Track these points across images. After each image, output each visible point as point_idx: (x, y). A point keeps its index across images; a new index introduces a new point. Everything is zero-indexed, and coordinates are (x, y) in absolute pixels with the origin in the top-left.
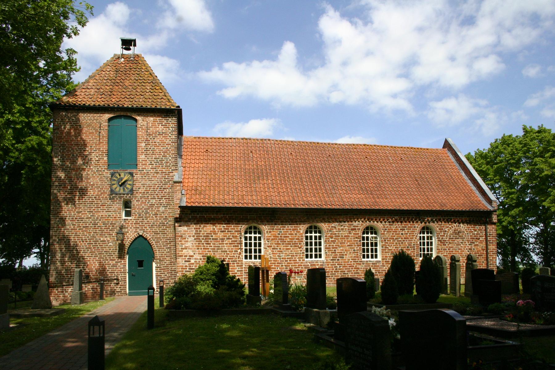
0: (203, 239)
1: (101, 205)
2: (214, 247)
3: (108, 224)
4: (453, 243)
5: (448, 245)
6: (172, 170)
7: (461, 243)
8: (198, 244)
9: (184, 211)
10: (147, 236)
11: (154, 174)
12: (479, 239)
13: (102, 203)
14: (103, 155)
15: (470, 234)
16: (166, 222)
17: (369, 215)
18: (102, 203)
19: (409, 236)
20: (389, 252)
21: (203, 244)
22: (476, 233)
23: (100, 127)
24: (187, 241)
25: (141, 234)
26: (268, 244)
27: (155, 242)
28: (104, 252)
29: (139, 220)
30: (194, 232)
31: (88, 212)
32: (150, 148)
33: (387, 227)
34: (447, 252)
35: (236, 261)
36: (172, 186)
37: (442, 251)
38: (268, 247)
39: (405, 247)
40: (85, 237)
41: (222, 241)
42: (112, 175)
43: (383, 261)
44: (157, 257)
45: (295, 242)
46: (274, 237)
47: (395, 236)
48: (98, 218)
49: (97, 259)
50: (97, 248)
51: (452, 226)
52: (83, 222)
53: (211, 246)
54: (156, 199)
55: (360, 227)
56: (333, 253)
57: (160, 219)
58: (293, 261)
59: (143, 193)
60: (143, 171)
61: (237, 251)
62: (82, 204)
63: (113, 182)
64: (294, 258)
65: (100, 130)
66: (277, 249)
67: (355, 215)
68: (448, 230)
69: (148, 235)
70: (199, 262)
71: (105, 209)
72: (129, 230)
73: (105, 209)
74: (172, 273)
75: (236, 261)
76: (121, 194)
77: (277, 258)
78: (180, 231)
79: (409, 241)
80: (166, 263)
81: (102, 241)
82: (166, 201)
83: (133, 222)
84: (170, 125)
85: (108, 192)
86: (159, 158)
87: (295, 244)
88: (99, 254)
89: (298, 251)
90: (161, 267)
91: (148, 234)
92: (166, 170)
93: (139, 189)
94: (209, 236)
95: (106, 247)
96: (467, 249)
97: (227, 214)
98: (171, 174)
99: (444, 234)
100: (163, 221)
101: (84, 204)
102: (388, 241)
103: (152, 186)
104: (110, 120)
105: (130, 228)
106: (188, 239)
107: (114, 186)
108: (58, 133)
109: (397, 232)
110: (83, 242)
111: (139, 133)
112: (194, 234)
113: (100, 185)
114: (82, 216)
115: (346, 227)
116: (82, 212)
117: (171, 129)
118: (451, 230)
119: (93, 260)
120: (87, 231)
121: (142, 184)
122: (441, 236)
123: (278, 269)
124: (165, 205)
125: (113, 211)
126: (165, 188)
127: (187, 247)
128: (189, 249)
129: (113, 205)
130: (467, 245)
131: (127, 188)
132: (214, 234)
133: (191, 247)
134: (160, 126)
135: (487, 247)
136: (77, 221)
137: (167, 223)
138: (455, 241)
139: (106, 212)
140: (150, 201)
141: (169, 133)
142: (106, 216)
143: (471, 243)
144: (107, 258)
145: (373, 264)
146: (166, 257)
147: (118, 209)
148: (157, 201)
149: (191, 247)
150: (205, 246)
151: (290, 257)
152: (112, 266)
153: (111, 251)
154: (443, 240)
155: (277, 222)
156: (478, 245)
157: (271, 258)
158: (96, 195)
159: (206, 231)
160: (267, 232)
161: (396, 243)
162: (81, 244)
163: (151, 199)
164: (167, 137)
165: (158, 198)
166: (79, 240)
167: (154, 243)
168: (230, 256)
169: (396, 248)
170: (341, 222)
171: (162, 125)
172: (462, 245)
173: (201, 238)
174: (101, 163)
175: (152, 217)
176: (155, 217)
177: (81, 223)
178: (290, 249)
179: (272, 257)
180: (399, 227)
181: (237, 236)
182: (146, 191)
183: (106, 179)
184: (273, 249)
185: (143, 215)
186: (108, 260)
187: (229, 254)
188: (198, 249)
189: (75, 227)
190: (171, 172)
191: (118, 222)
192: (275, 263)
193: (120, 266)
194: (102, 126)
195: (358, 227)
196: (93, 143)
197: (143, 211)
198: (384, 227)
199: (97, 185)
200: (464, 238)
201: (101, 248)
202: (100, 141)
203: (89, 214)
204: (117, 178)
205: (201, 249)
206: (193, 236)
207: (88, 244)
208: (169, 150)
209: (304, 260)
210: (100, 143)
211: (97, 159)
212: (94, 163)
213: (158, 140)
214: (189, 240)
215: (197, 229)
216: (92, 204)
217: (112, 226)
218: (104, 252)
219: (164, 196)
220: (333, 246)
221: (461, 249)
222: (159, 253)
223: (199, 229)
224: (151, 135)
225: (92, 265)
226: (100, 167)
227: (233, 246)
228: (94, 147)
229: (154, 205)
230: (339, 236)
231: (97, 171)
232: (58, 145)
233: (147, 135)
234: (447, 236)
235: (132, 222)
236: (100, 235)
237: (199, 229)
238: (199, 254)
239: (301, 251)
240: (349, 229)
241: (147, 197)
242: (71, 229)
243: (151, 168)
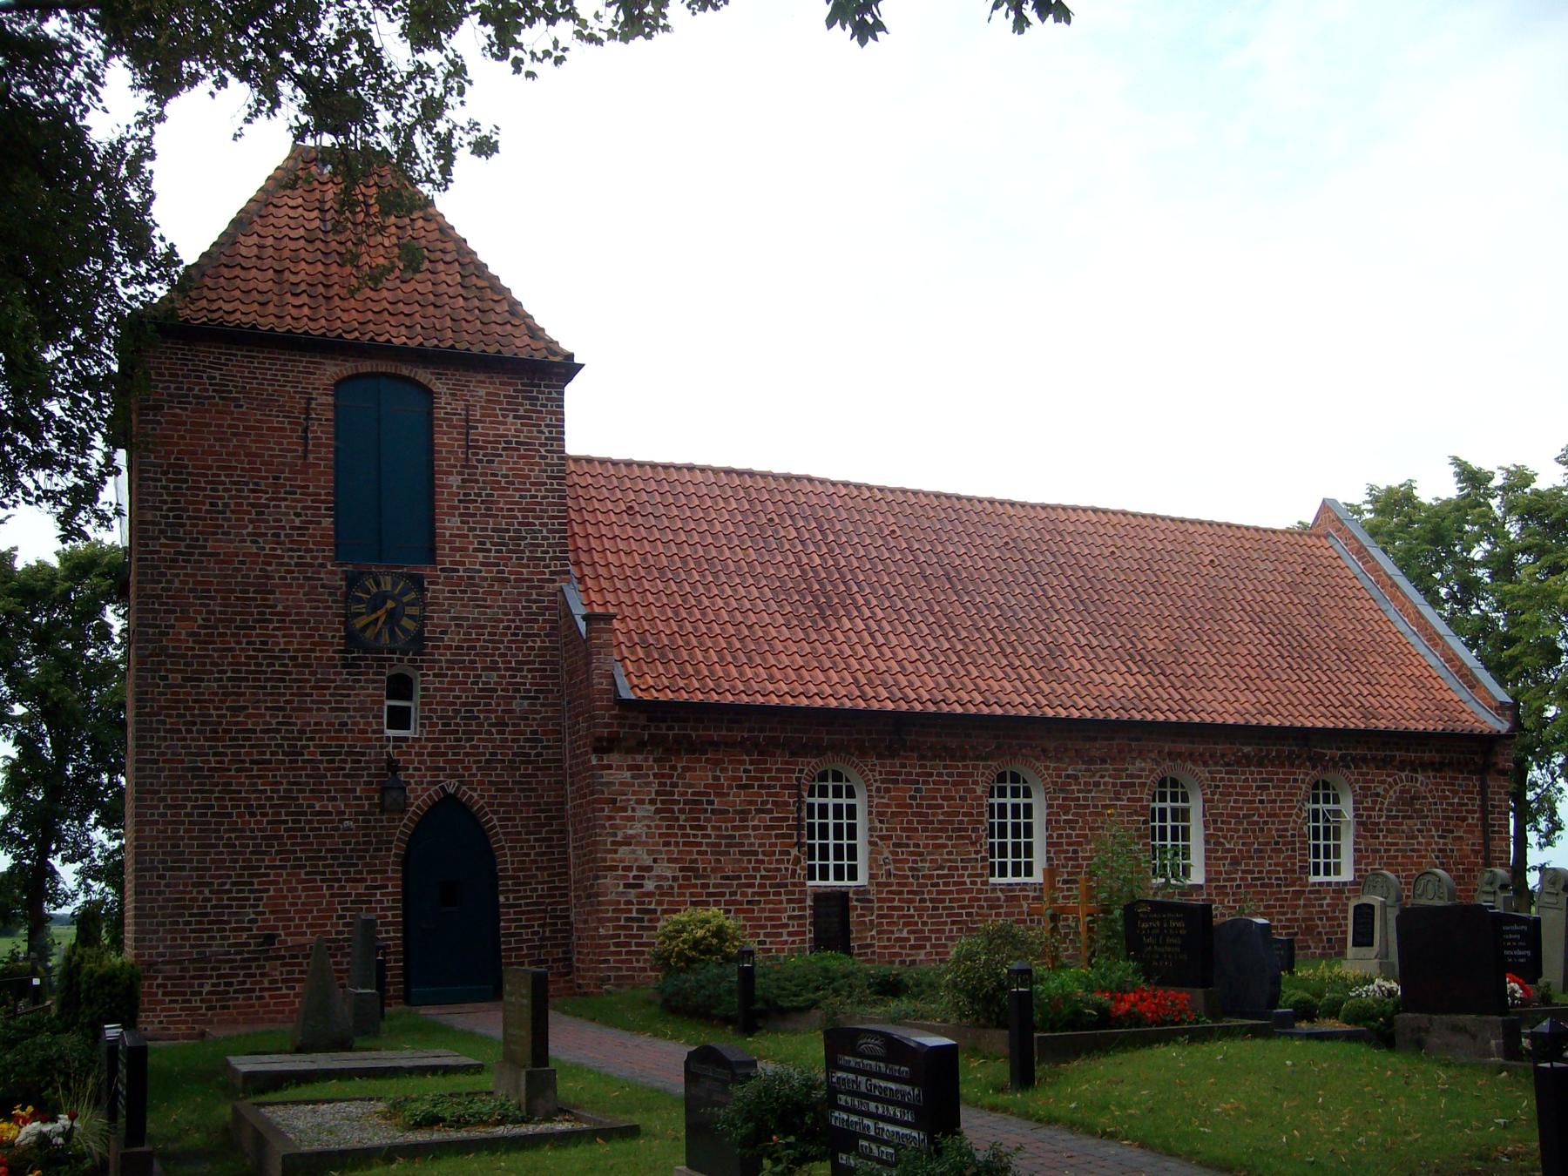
0: (682, 811)
1: (311, 688)
2: (717, 837)
3: (340, 754)
4: (1397, 831)
6: (552, 573)
7: (1419, 830)
8: (668, 827)
9: (626, 718)
10: (471, 797)
11: (493, 586)
12: (1465, 819)
13: (317, 680)
14: (319, 509)
15: (1442, 804)
16: (533, 752)
17: (1173, 742)
18: (317, 680)
19: (1281, 808)
20: (1226, 858)
21: (682, 827)
22: (1456, 800)
23: (307, 410)
24: (632, 819)
25: (451, 790)
26: (881, 829)
27: (500, 820)
28: (328, 851)
29: (444, 740)
30: (655, 787)
31: (267, 708)
32: (479, 495)
33: (1222, 779)
35: (786, 885)
36: (551, 628)
37: (1368, 857)
38: (881, 838)
39: (1268, 843)
40: (260, 799)
41: (741, 820)
42: (352, 580)
43: (1209, 887)
44: (506, 870)
45: (961, 822)
46: (898, 806)
47: (1241, 809)
48: (304, 732)
49: (303, 877)
50: (302, 837)
51: (1395, 780)
52: (251, 746)
53: (709, 836)
54: (499, 669)
55: (1147, 777)
56: (1070, 859)
57: (513, 740)
58: (955, 884)
59: (457, 648)
60: (458, 571)
61: (789, 853)
62: (247, 680)
63: (355, 608)
64: (959, 876)
65: (307, 419)
66: (907, 846)
67: (1132, 740)
68: (1385, 790)
69: (475, 795)
70: (672, 887)
71: (329, 702)
72: (412, 776)
73: (329, 702)
74: (556, 924)
75: (786, 885)
77: (907, 877)
79: (1281, 822)
80: (536, 890)
81: (319, 813)
82: (534, 678)
83: (426, 747)
84: (543, 419)
85: (336, 640)
86: (508, 531)
87: (959, 830)
88: (308, 859)
89: (969, 853)
90: (520, 905)
91: (475, 790)
92: (532, 573)
93: (442, 632)
94: (701, 802)
95: (332, 836)
96: (1433, 850)
97: (762, 730)
98: (549, 587)
99: (1375, 802)
100: (524, 747)
101: (254, 680)
102: (1222, 822)
103: (485, 627)
104: (341, 384)
105: (416, 769)
106: (633, 810)
107: (360, 623)
108: (159, 423)
109: (1247, 795)
110: (253, 815)
111: (441, 439)
112: (653, 796)
113: (309, 614)
114: (247, 724)
115: (1106, 779)
116: (246, 708)
117: (546, 430)
118: (1391, 793)
119: (286, 882)
120: (267, 777)
121: (452, 619)
123: (912, 911)
124: (529, 691)
125: (355, 710)
126: (528, 635)
127: (632, 836)
128: (638, 844)
129: (353, 689)
130: (1433, 837)
131: (405, 631)
132: (717, 794)
133: (644, 838)
134: (510, 419)
135: (1486, 845)
136: (232, 739)
137: (539, 755)
138: (1402, 824)
139: (332, 710)
140: (480, 676)
141: (541, 445)
142: (332, 724)
143: (1443, 831)
144: (335, 873)
146: (537, 869)
147: (373, 702)
148: (504, 677)
149: (644, 838)
150: (687, 836)
151: (946, 872)
152: (352, 902)
153: (351, 850)
154: (1372, 824)
155: (907, 758)
156: (1460, 838)
157: (889, 874)
158: (296, 651)
159: (691, 786)
160: (878, 790)
161: (1246, 831)
162: (243, 823)
163: (484, 669)
164: (534, 457)
165: (507, 669)
166: (239, 807)
167: (495, 822)
168: (765, 869)
169: (1243, 844)
170: (1092, 761)
171: (515, 417)
172: (1421, 839)
173: (676, 808)
174: (313, 536)
175: (489, 732)
176: (499, 732)
177: (244, 746)
178: (945, 846)
179: (893, 871)
180: (1254, 780)
181: (787, 804)
182: (465, 640)
183: (330, 594)
184: (895, 845)
185: (457, 725)
186: (339, 880)
187: (762, 862)
188: (667, 844)
189: (222, 762)
190: (548, 581)
191: (375, 747)
192: (901, 893)
193: (381, 902)
194: (313, 406)
195: (1140, 777)
196: (283, 464)
197: (457, 712)
198: (1213, 779)
199: (297, 614)
201: (315, 837)
202: (305, 457)
203: (271, 716)
204: (368, 592)
205: (677, 844)
206: (652, 802)
207: (269, 822)
208: (540, 504)
209: (986, 883)
210: (307, 466)
211: (297, 523)
212: (287, 535)
213: (504, 467)
214: (638, 814)
215: (663, 776)
216: (283, 680)
217: (354, 762)
218: (328, 851)
219: (528, 663)
220: (1068, 836)
222: (512, 855)
223: (671, 776)
224: (481, 448)
225: (285, 897)
226: (307, 551)
227: (777, 836)
228: (286, 479)
229: (495, 690)
230: (1087, 807)
231: (297, 565)
232: (161, 466)
233: (468, 447)
234: (1380, 810)
235: (421, 747)
236: (312, 791)
237: (671, 776)
238: (670, 861)
239: (977, 852)
240: (1114, 785)
241: (471, 662)
242: (210, 769)
243: (482, 564)
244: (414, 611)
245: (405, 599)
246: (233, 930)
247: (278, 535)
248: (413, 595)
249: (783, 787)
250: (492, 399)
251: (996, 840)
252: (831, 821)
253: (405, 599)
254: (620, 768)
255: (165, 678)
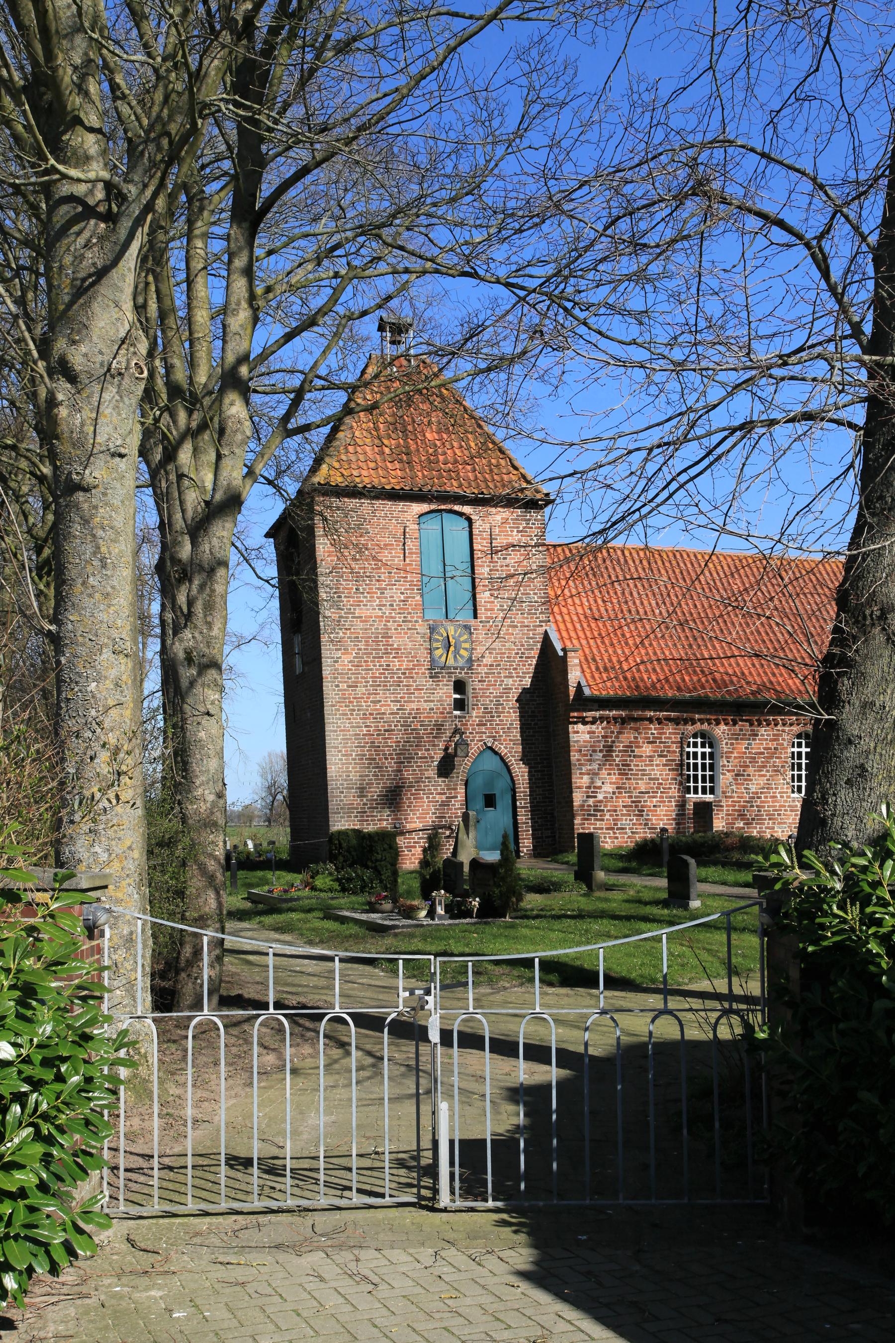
21: (617, 765)
25: (489, 745)
76: (449, 668)
78: (577, 741)
110: (386, 759)
131: (462, 656)
134: (515, 533)
157: (733, 791)
181: (675, 752)
188: (609, 774)
206: (601, 751)
209: (789, 797)
244: (467, 645)
245: (462, 639)
246: (379, 820)
247: (392, 605)
248: (466, 637)
249: (673, 742)
250: (505, 521)
251: (796, 773)
252: (699, 761)
253: (462, 639)
254: (583, 732)
255: (337, 686)
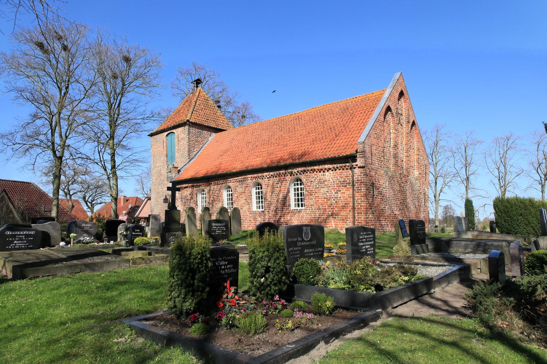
4: (319, 192)
5: (314, 194)
7: (327, 192)
15: (336, 182)
34: (314, 201)
51: (317, 176)
68: (314, 180)
104: (167, 136)
118: (316, 180)
122: (308, 186)
135: (353, 194)
138: (320, 190)
145: (259, 213)
154: (310, 191)
156: (344, 193)
200: (330, 187)
221: (327, 198)
234: (313, 186)
